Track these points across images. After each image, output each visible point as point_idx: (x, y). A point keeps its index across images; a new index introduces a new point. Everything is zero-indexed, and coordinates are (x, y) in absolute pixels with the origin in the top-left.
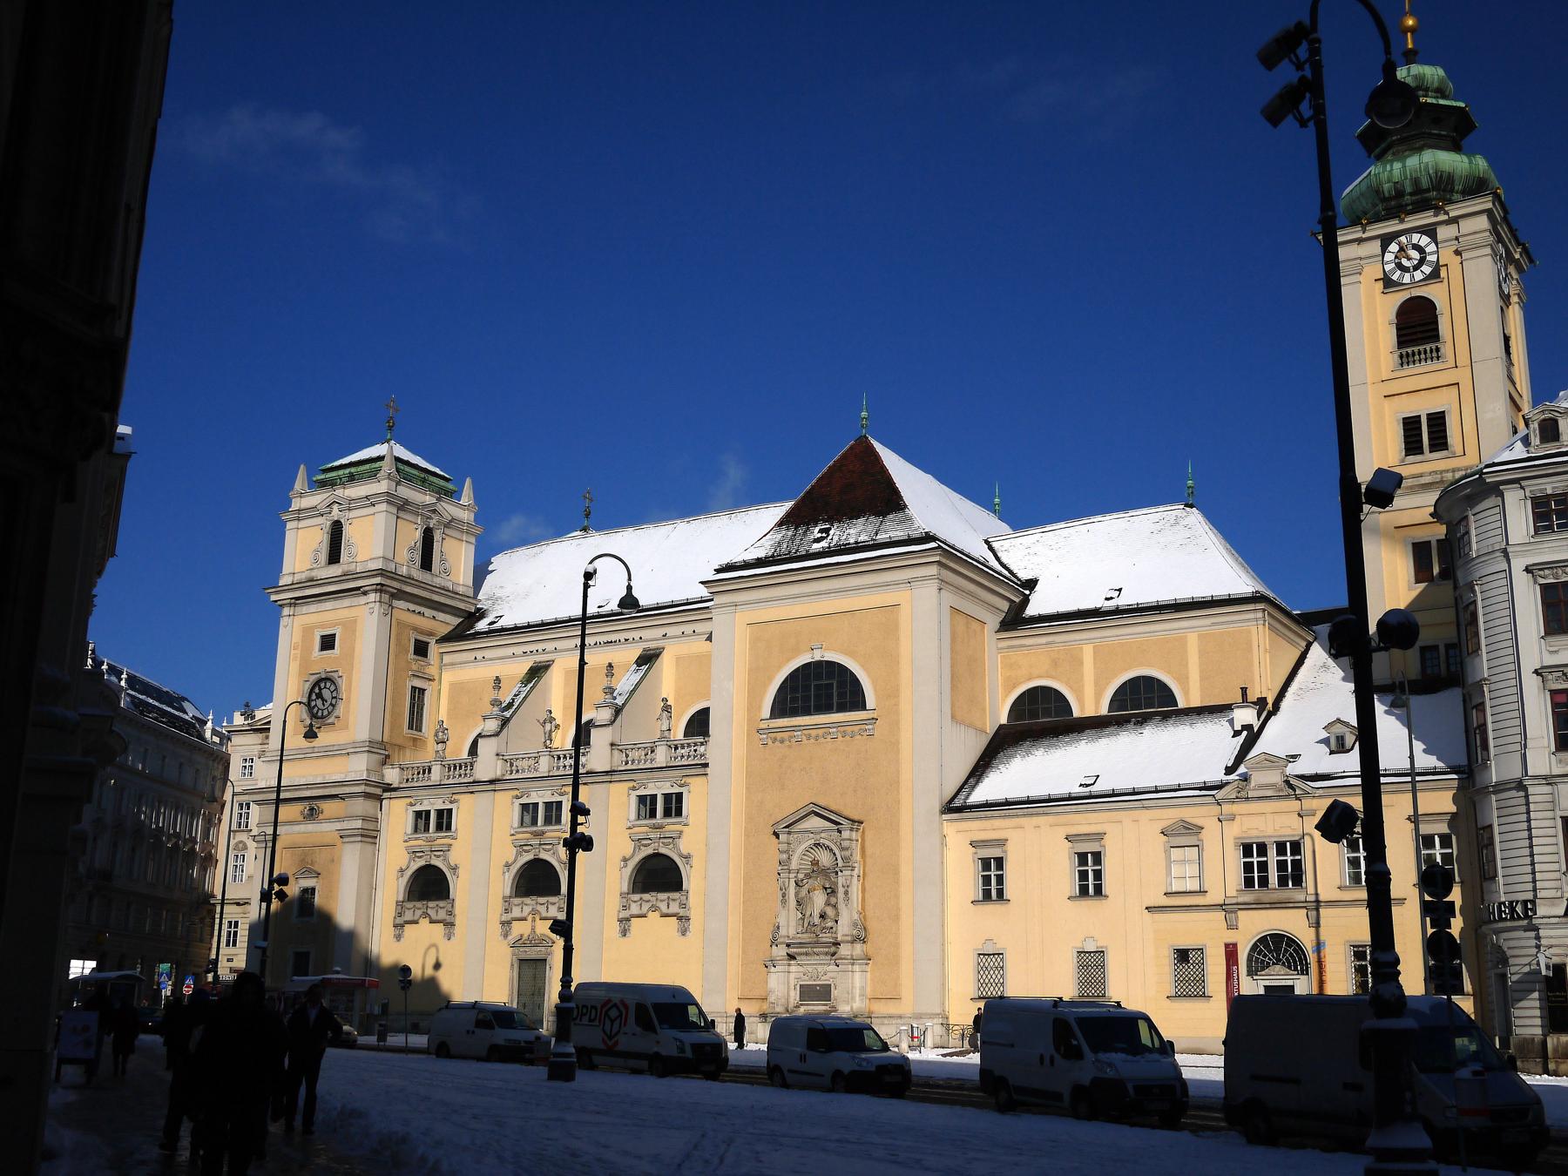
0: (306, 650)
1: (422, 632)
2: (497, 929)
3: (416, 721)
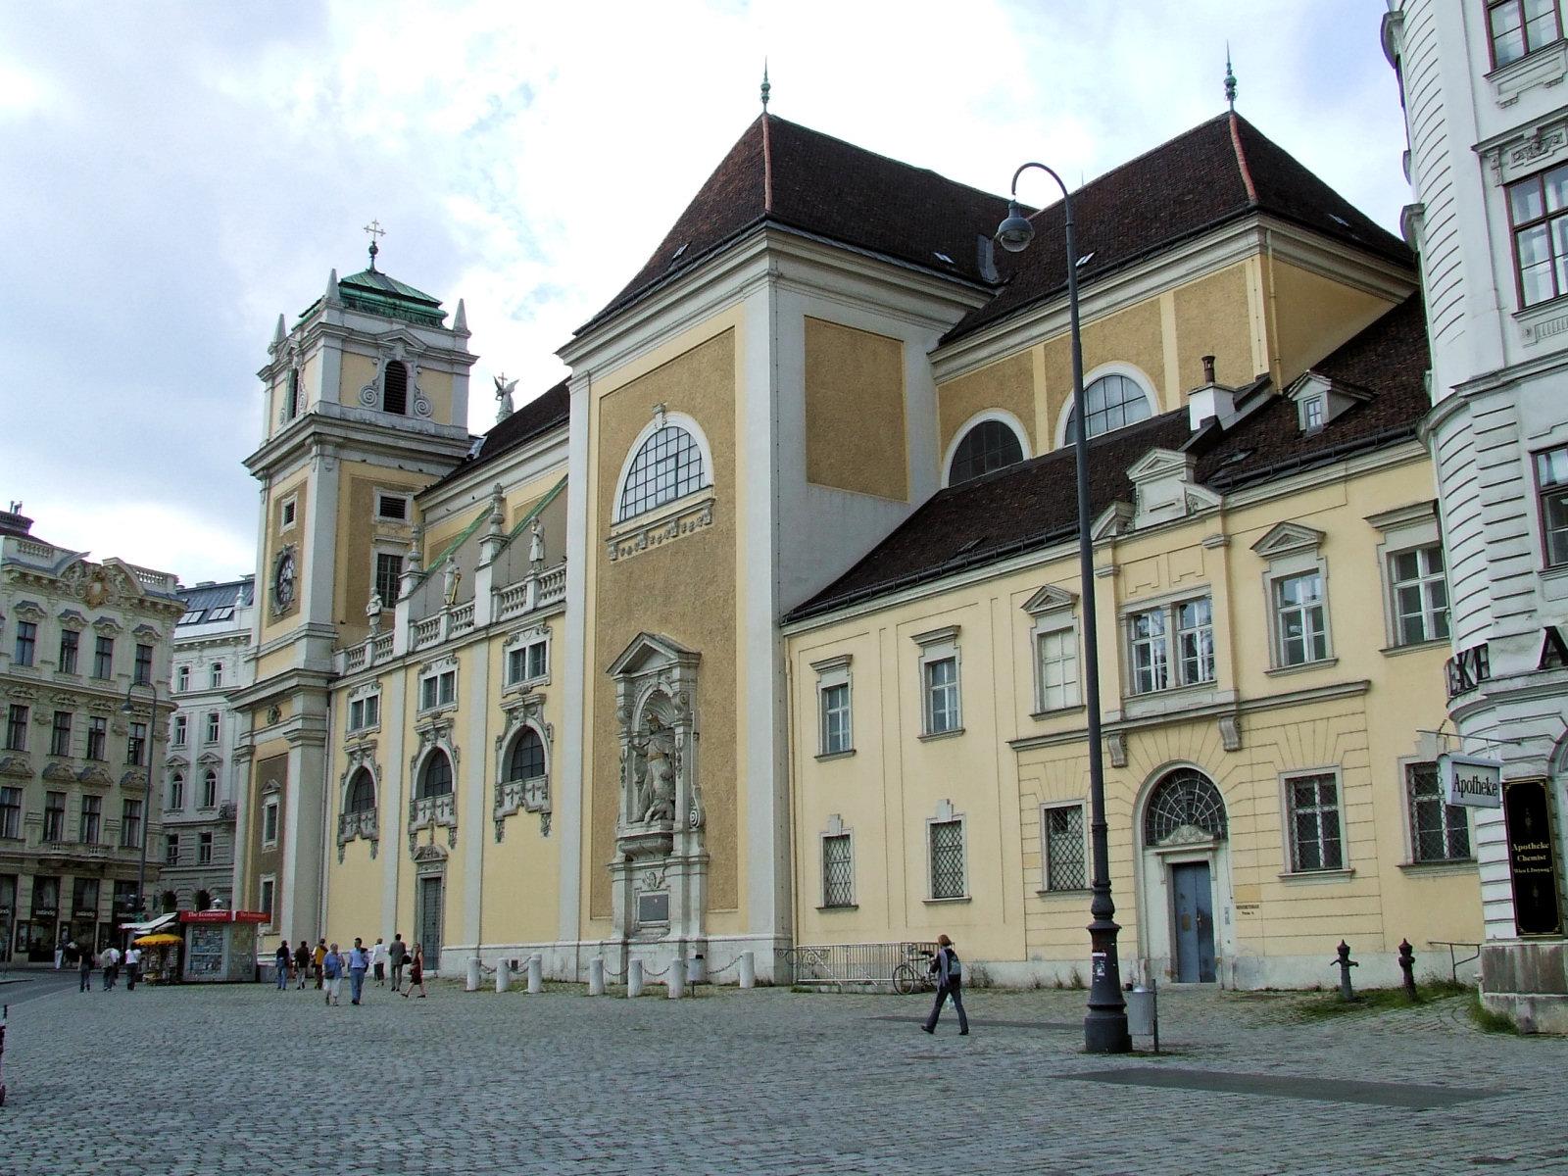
0: (277, 522)
2: (406, 838)
3: (389, 593)
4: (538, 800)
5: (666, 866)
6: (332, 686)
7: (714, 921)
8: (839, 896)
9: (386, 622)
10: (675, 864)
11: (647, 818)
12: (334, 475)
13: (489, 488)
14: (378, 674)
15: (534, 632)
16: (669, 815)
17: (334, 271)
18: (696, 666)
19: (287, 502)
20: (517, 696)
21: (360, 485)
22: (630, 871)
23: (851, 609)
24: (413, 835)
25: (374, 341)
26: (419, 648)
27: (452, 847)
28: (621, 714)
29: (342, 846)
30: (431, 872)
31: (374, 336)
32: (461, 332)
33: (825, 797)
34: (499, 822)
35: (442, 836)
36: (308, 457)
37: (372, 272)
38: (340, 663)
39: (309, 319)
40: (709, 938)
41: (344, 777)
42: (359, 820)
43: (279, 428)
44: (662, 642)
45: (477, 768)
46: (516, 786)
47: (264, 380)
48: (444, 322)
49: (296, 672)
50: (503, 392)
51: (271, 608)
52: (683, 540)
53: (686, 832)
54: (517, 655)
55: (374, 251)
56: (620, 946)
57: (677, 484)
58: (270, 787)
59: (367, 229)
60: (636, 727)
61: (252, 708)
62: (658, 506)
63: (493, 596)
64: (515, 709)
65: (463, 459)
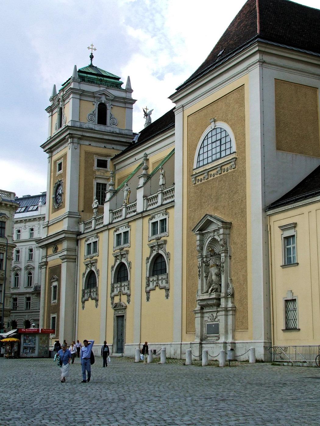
0: (55, 171)
1: (101, 155)
3: (101, 200)
4: (164, 284)
5: (218, 312)
6: (78, 237)
7: (238, 335)
8: (292, 325)
9: (100, 211)
10: (221, 311)
11: (209, 292)
12: (78, 151)
13: (142, 155)
14: (97, 232)
15: (161, 214)
16: (219, 290)
17: (76, 66)
18: (230, 228)
19: (59, 162)
20: (155, 241)
21: (89, 155)
22: (202, 313)
23: (296, 204)
24: (112, 298)
25: (93, 95)
26: (114, 221)
27: (129, 303)
28: (198, 248)
29: (83, 302)
30: (120, 313)
31: (93, 93)
32: (129, 90)
33: (285, 282)
34: (148, 293)
35: (124, 298)
36: (66, 145)
37: (91, 66)
38: (82, 228)
39: (65, 87)
40: (236, 342)
41: (84, 274)
42: (90, 292)
43: (55, 132)
44: (215, 218)
45: (138, 271)
46: (155, 278)
47: (49, 112)
48: (122, 86)
49: (64, 232)
50: (147, 115)
51: (53, 206)
52: (223, 175)
53: (226, 298)
54: (155, 224)
55: (92, 57)
56: (198, 345)
57: (221, 152)
58: (54, 278)
59: (89, 48)
60: (205, 253)
61: (47, 246)
62: (213, 161)
63: (144, 199)
64: (154, 246)
65: (131, 143)
